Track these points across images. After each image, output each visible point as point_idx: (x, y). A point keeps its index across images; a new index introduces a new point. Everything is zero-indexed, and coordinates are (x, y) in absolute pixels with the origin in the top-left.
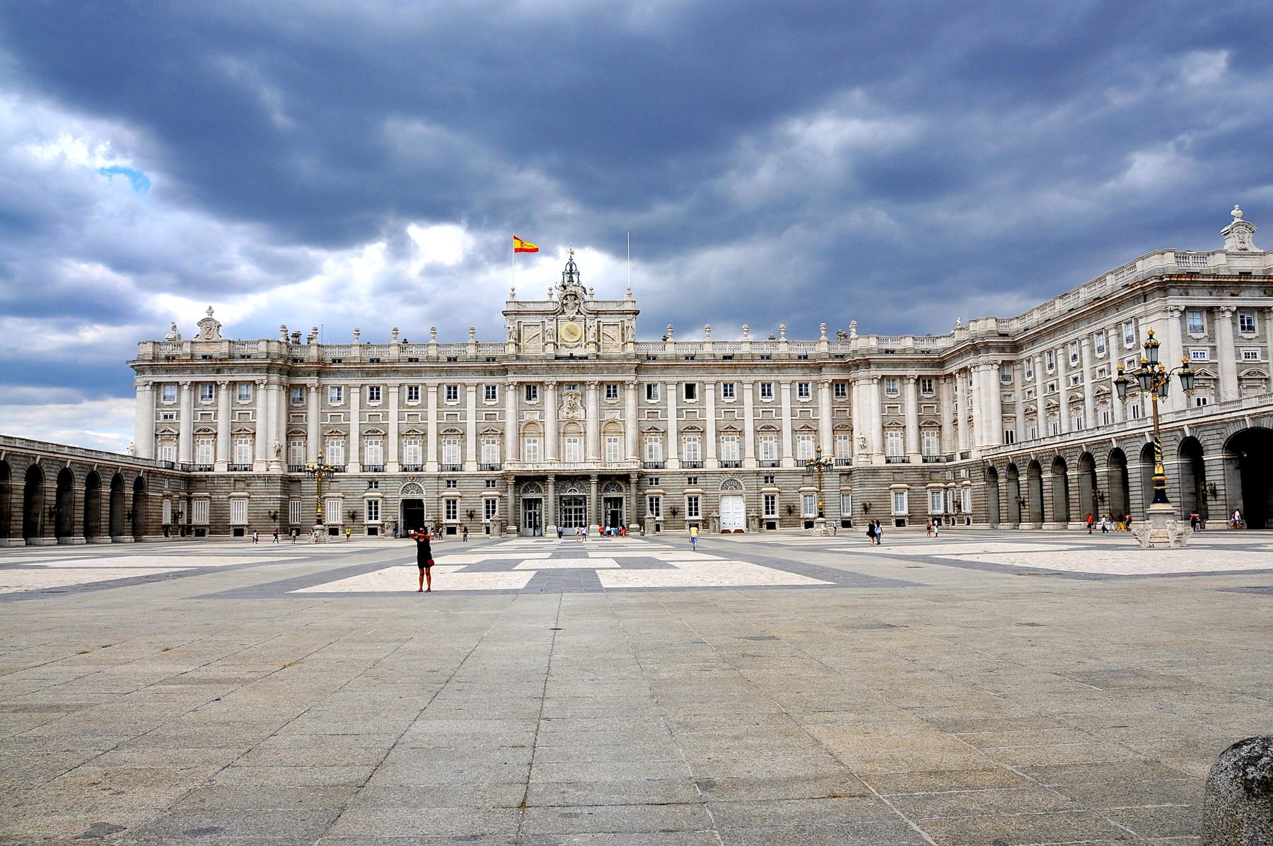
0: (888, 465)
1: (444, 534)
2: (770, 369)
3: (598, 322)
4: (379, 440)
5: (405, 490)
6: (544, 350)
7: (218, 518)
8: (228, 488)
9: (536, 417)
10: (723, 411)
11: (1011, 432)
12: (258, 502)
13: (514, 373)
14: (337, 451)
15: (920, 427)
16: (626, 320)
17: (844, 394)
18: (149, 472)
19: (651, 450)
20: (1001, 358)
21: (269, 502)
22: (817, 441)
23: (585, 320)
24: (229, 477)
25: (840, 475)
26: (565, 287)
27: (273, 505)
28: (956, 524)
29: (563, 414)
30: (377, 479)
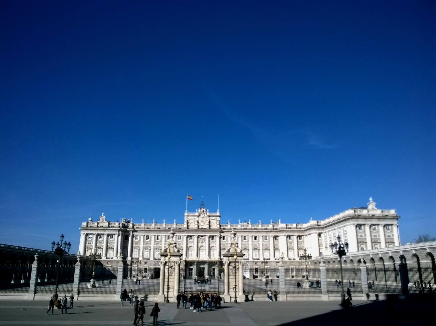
3: (210, 218)
4: (148, 250)
5: (155, 265)
6: (194, 226)
9: (192, 245)
11: (322, 253)
13: (187, 233)
14: (136, 254)
15: (298, 250)
17: (277, 239)
18: (87, 260)
22: (270, 253)
24: (106, 260)
26: (201, 209)
29: (200, 244)
30: (147, 262)
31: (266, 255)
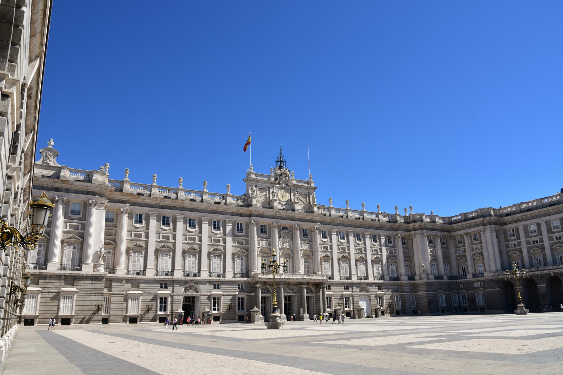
0: (436, 280)
1: (212, 321)
2: (376, 228)
5: (186, 290)
7: (47, 309)
8: (59, 284)
10: (357, 248)
12: (85, 297)
14: (138, 260)
16: (310, 193)
19: (325, 269)
20: (498, 227)
21: (93, 297)
23: (290, 189)
25: (410, 285)
27: (98, 299)
28: (468, 310)
31: (392, 271)
